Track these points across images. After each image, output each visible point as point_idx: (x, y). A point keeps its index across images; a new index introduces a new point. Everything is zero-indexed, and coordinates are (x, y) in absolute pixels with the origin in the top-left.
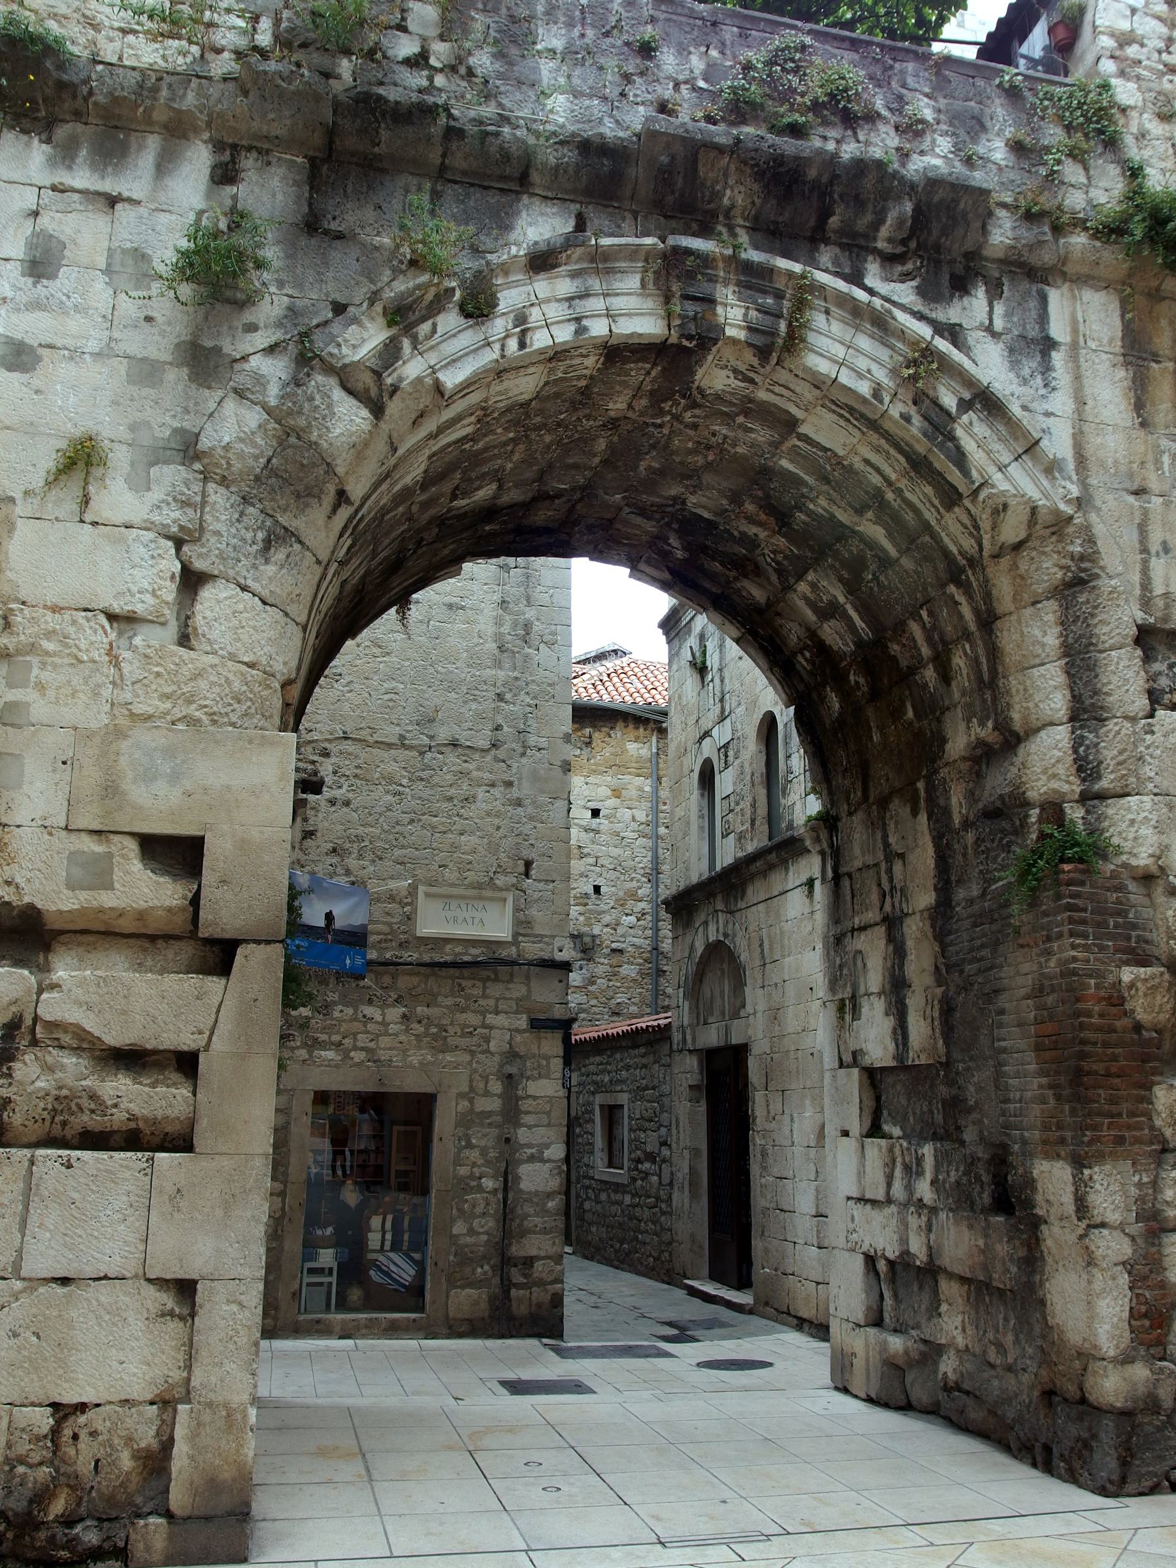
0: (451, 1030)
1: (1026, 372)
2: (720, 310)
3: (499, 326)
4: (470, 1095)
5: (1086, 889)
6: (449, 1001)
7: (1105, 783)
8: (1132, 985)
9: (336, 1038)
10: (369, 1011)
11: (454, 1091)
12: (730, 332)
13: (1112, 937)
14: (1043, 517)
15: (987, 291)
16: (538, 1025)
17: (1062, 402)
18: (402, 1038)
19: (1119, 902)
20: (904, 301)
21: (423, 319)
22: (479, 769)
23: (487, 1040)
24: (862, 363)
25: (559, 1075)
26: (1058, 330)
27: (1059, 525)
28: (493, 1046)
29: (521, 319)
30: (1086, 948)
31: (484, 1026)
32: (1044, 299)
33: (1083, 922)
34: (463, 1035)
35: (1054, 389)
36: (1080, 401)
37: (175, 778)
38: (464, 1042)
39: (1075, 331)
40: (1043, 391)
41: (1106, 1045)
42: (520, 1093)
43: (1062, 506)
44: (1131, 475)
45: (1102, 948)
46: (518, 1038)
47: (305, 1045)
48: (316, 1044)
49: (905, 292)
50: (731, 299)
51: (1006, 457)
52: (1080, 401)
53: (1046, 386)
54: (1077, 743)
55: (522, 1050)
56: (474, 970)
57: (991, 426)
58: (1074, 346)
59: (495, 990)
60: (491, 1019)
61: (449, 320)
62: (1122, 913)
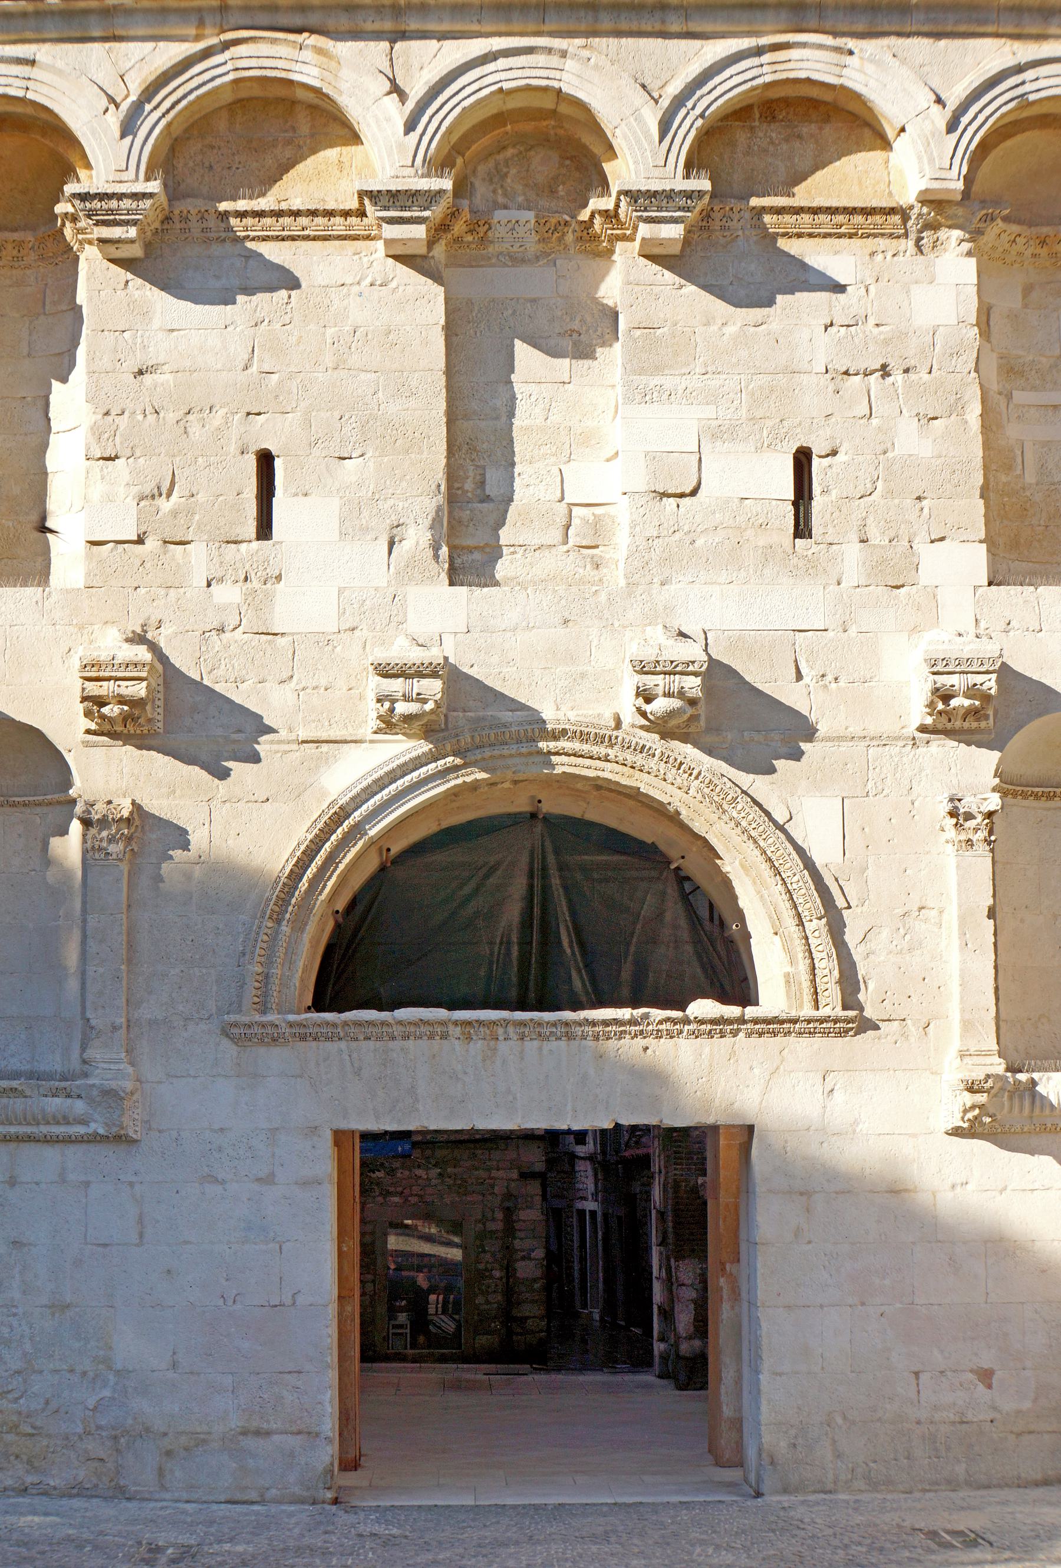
4: (483, 1220)
6: (468, 1164)
8: (702, 1185)
9: (400, 1189)
10: (419, 1172)
11: (473, 1219)
16: (524, 1176)
23: (492, 1186)
25: (539, 1207)
28: (496, 1190)
31: (490, 1178)
42: (514, 1218)
46: (513, 1184)
48: (389, 1193)
55: (515, 1193)
59: (496, 1155)
60: (494, 1173)
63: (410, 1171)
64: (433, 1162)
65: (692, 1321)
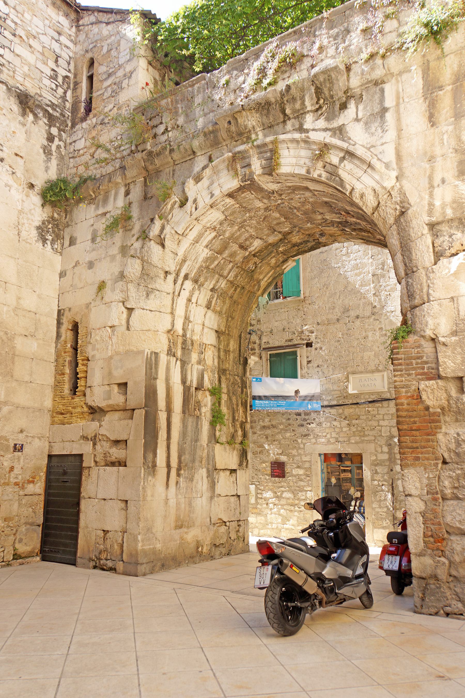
0: (366, 428)
6: (364, 417)
9: (324, 434)
10: (335, 423)
17: (391, 135)
18: (348, 432)
20: (319, 127)
22: (369, 325)
23: (381, 431)
34: (371, 430)
36: (400, 130)
38: (371, 433)
40: (381, 135)
47: (314, 437)
51: (360, 173)
52: (400, 130)
56: (373, 404)
59: (382, 411)
60: (382, 423)
63: (331, 423)
64: (344, 417)
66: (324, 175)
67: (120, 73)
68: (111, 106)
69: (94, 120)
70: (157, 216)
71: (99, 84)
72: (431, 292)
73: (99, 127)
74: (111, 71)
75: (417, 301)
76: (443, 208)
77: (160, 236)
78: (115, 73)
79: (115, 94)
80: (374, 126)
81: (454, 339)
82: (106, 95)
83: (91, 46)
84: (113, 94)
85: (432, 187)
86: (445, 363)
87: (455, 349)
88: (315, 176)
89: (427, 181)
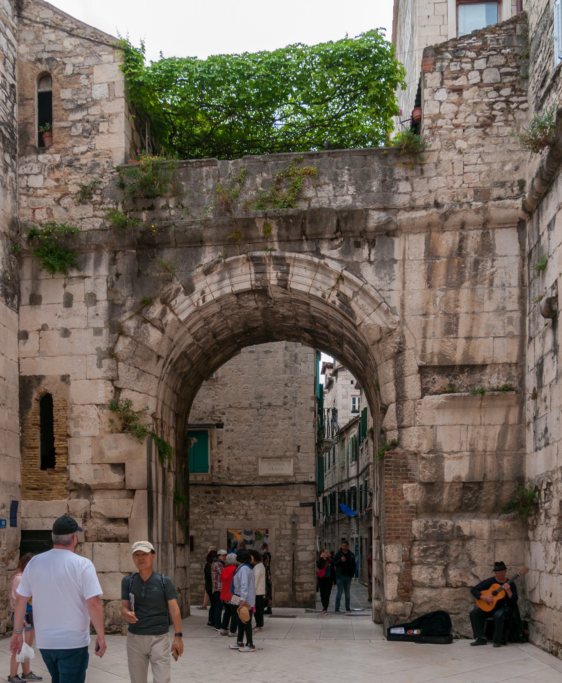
1: (383, 275)
2: (268, 275)
3: (196, 296)
5: (393, 459)
7: (405, 423)
8: (406, 489)
12: (272, 282)
13: (400, 474)
14: (385, 330)
15: (369, 246)
17: (397, 284)
19: (404, 462)
21: (173, 300)
24: (318, 285)
26: (397, 255)
27: (390, 332)
29: (203, 292)
30: (391, 478)
32: (393, 243)
33: (390, 470)
35: (394, 279)
37: (116, 448)
39: (404, 254)
41: (395, 508)
43: (390, 326)
44: (423, 308)
45: (396, 478)
48: (227, 514)
49: (335, 254)
50: (272, 270)
53: (390, 279)
54: (397, 409)
57: (365, 300)
58: (404, 260)
61: (181, 297)
62: (406, 466)
65: (396, 588)
66: (338, 303)
67: (95, 110)
68: (83, 148)
69: (58, 158)
70: (158, 299)
71: (63, 112)
72: (417, 419)
73: (67, 170)
74: (79, 102)
75: (405, 423)
76: (432, 357)
77: (161, 320)
78: (87, 108)
79: (87, 134)
80: (383, 272)
81: (431, 455)
82: (74, 132)
83: (45, 56)
84: (85, 134)
85: (425, 337)
86: (423, 471)
87: (431, 463)
88: (330, 301)
89: (421, 331)
